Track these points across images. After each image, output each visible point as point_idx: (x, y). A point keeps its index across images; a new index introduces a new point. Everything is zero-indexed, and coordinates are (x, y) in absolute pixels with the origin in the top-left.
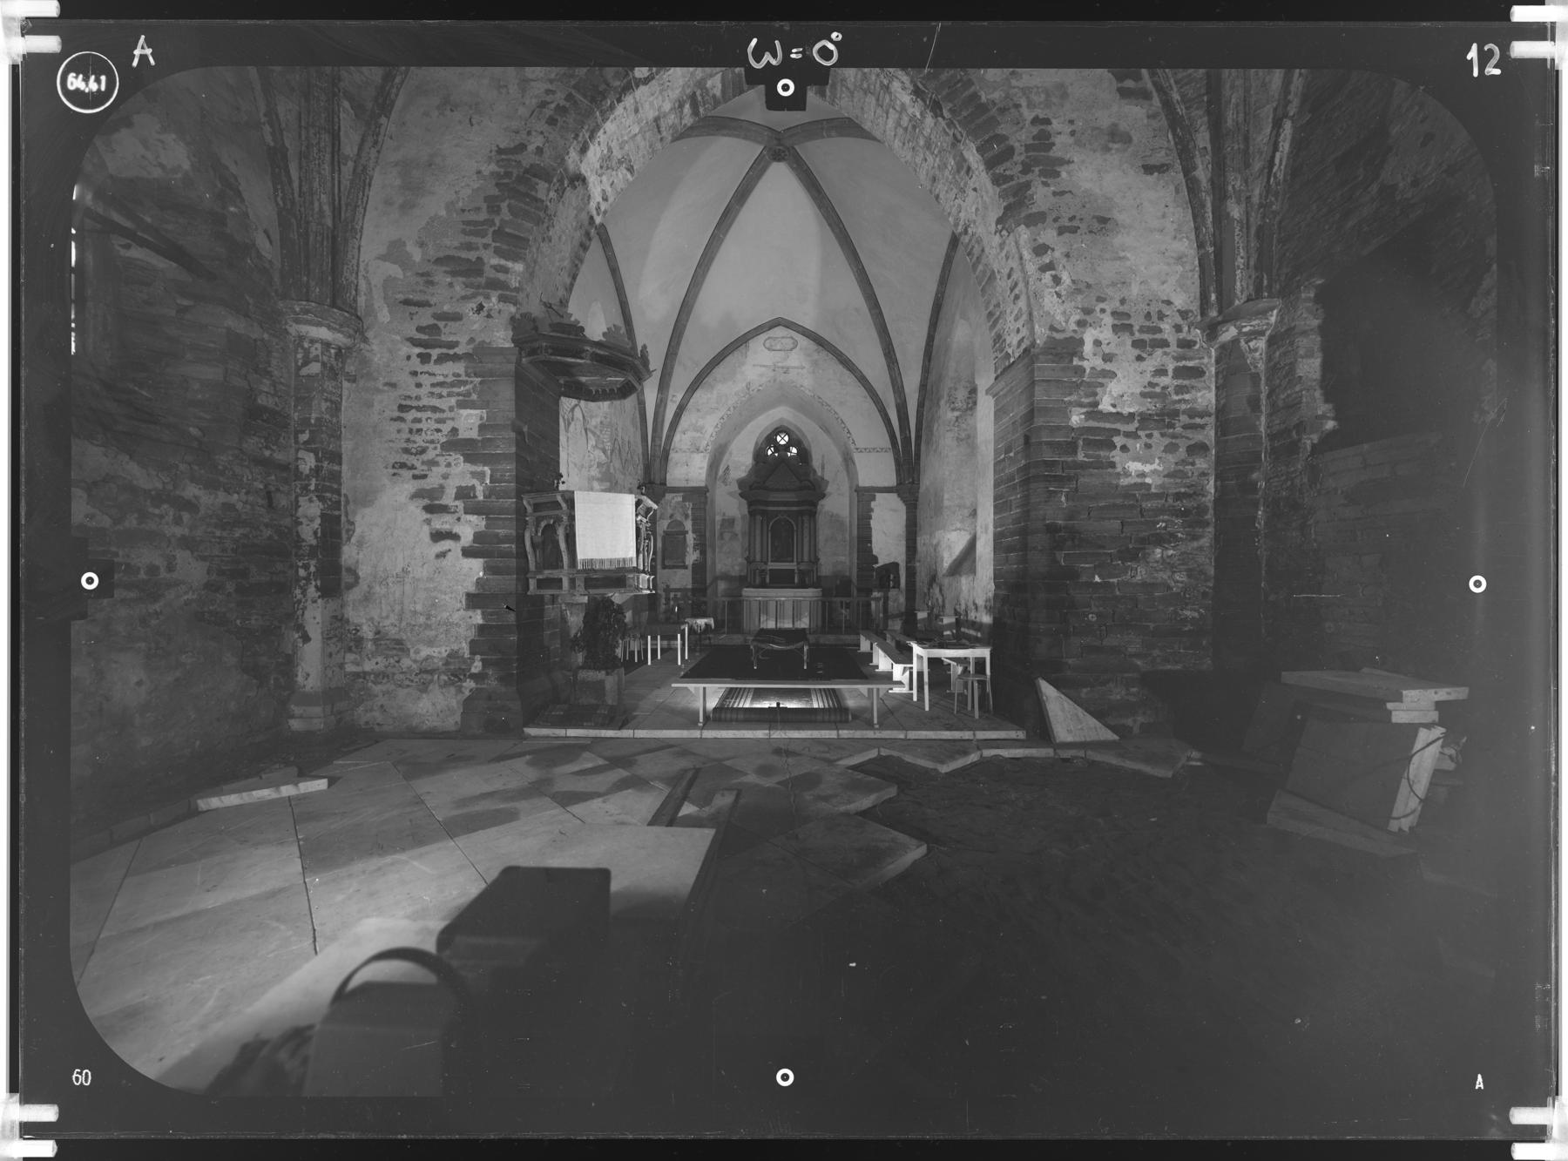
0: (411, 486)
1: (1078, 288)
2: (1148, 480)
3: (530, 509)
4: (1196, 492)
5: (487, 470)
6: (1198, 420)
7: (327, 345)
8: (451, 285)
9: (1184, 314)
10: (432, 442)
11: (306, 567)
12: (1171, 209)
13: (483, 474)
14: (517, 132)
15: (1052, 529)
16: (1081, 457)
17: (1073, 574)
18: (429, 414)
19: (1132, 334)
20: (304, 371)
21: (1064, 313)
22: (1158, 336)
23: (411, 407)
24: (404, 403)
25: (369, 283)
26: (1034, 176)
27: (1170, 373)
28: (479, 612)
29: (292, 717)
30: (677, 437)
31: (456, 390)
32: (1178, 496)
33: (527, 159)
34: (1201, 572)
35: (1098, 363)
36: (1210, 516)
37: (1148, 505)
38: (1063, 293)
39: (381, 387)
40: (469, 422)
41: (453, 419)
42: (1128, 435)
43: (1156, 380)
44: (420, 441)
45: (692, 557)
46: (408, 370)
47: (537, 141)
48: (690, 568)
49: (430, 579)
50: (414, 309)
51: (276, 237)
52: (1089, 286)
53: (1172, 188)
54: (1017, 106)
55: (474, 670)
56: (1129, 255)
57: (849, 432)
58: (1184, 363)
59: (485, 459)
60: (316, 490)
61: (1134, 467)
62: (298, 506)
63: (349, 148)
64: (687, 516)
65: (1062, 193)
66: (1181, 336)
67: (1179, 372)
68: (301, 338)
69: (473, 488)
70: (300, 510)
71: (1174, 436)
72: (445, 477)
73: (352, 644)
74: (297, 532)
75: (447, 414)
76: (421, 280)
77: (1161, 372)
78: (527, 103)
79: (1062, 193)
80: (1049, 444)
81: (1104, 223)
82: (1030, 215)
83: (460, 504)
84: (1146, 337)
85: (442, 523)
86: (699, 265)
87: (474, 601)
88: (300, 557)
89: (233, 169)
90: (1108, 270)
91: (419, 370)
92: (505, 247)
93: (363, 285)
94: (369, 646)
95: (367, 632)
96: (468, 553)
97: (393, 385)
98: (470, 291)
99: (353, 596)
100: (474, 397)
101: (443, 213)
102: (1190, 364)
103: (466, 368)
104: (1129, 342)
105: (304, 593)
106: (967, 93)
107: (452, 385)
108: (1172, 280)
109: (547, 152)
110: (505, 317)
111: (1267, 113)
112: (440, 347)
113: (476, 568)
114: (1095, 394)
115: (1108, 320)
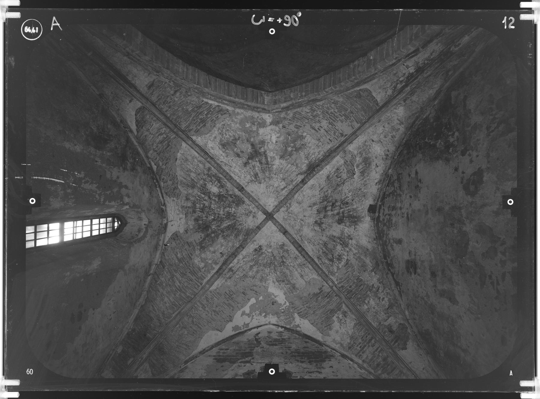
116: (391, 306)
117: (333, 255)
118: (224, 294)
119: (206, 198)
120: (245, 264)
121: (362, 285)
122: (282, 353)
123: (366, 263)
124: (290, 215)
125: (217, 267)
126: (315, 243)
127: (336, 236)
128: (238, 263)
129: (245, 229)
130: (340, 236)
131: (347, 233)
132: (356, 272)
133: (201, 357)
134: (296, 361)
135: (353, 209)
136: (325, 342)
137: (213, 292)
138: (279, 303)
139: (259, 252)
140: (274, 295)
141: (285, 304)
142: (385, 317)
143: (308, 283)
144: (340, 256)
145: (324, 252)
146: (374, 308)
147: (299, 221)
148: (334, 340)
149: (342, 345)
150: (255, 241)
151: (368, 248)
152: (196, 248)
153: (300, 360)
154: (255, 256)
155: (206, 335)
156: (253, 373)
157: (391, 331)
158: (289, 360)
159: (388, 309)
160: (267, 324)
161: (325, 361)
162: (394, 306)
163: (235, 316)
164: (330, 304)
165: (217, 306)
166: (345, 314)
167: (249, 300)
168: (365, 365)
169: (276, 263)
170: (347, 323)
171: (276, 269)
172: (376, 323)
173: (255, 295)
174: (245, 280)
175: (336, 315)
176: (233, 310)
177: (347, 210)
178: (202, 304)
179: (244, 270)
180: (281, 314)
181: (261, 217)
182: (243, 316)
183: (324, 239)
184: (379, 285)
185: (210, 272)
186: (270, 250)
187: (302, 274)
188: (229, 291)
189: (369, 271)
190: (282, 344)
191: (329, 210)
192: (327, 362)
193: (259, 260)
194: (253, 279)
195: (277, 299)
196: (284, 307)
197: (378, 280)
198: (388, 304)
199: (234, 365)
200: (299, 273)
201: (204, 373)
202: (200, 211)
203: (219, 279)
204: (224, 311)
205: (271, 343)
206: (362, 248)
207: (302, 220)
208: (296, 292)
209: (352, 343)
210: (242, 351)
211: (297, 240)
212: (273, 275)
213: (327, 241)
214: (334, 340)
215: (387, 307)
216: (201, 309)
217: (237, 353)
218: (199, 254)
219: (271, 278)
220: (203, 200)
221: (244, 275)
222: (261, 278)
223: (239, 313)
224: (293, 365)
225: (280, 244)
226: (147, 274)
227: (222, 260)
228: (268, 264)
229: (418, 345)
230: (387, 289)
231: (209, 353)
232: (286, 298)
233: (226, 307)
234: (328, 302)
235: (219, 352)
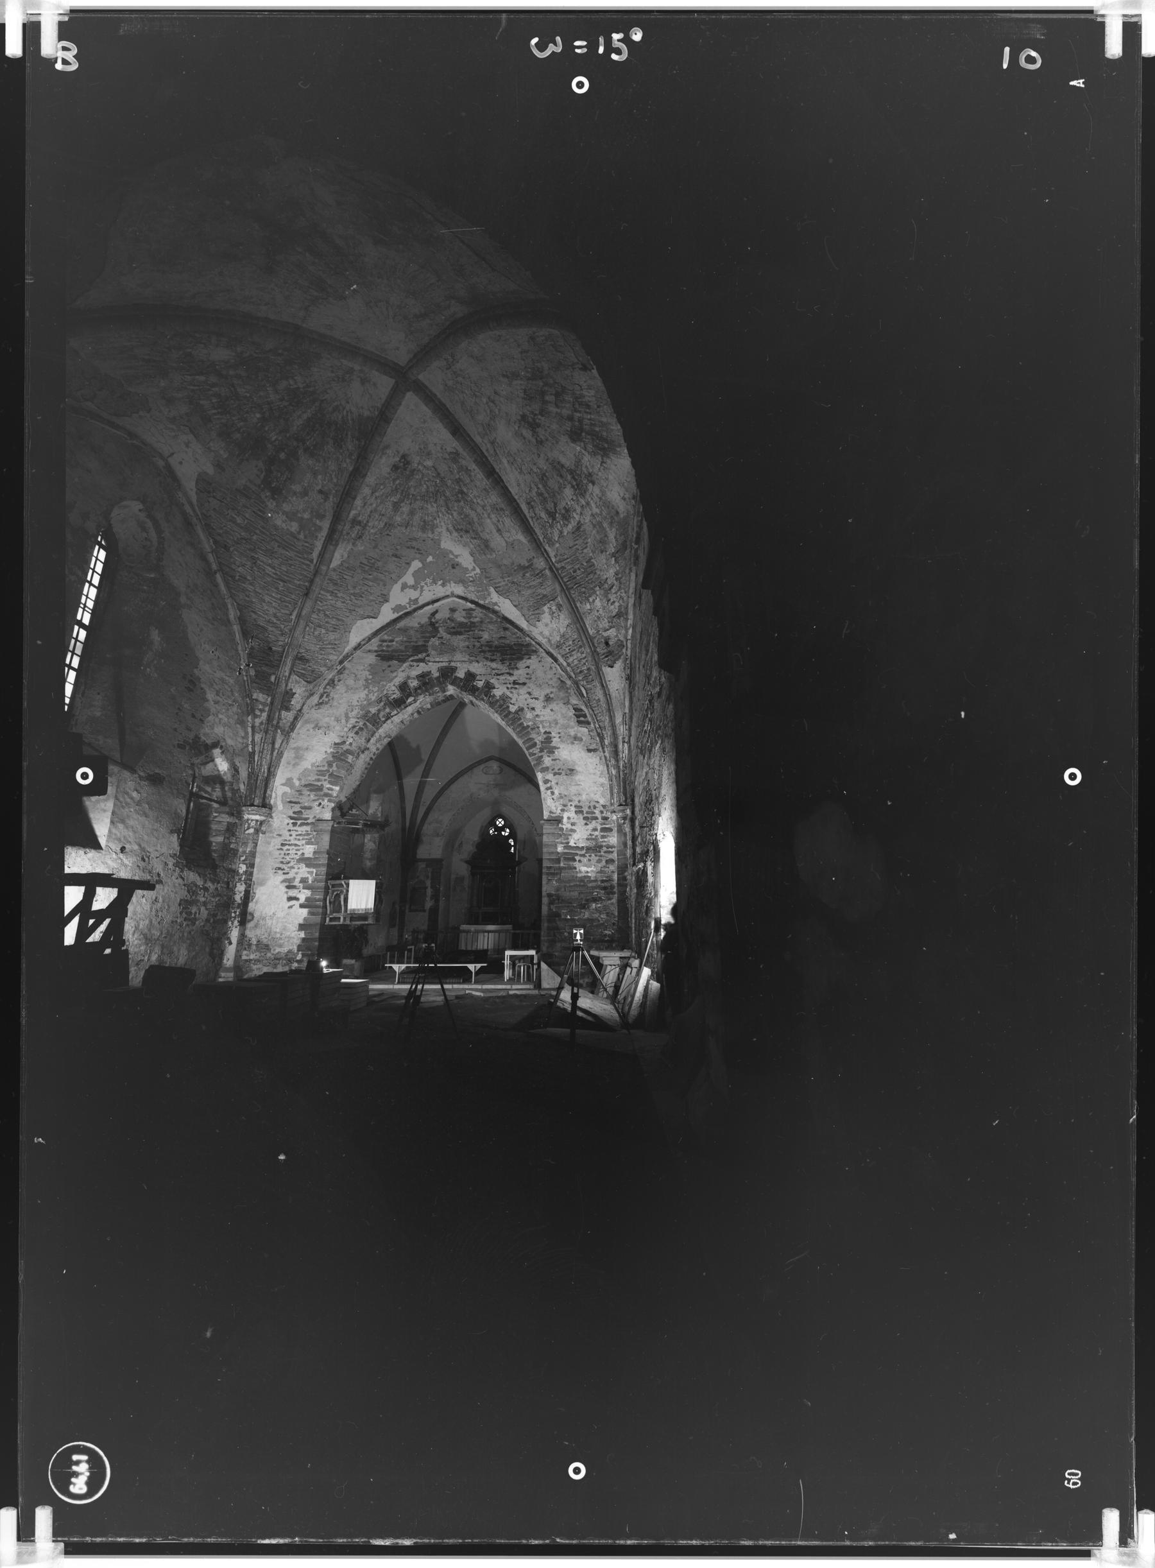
0: (281, 877)
1: (561, 797)
2: (589, 875)
3: (330, 887)
4: (610, 880)
5: (314, 870)
6: (610, 849)
7: (257, 821)
8: (309, 795)
9: (604, 806)
10: (293, 859)
11: (235, 912)
12: (599, 766)
13: (312, 872)
14: (343, 737)
15: (549, 895)
16: (562, 865)
17: (558, 915)
18: (293, 847)
19: (583, 814)
20: (247, 832)
21: (555, 806)
22: (593, 815)
23: (286, 844)
24: (284, 842)
25: (276, 794)
26: (544, 754)
27: (599, 830)
28: (303, 932)
29: (220, 977)
30: (425, 828)
31: (306, 837)
32: (602, 881)
33: (346, 747)
34: (612, 914)
35: (569, 826)
36: (615, 890)
37: (590, 885)
38: (555, 798)
39: (275, 836)
40: (309, 851)
41: (303, 849)
42: (581, 855)
43: (593, 833)
44: (288, 858)
45: (429, 904)
46: (287, 829)
47: (351, 740)
48: (427, 911)
49: (284, 917)
50: (293, 805)
51: (246, 783)
52: (565, 796)
53: (598, 758)
54: (538, 727)
55: (298, 958)
56: (581, 783)
57: (533, 824)
58: (604, 826)
59: (314, 866)
60: (245, 880)
61: (584, 869)
62: (236, 887)
63: (277, 746)
64: (428, 877)
65: (555, 760)
66: (603, 815)
67: (603, 830)
68: (248, 820)
69: (308, 878)
70: (237, 888)
71: (601, 856)
72: (297, 873)
73: (247, 947)
74: (234, 898)
75: (303, 847)
76: (297, 793)
77: (595, 830)
78: (348, 726)
79: (555, 760)
80: (549, 859)
81: (571, 771)
82: (543, 768)
83: (301, 885)
84: (589, 816)
85: (292, 893)
86: (441, 734)
87: (302, 927)
88: (233, 908)
89: (238, 765)
90: (573, 790)
91: (292, 829)
92: (333, 780)
93: (274, 795)
94: (254, 947)
95: (254, 941)
96: (302, 906)
97: (280, 835)
98: (316, 798)
99: (250, 925)
100: (313, 840)
101: (310, 767)
102: (607, 826)
103: (311, 828)
104: (582, 818)
105: (232, 924)
106: (519, 723)
107: (304, 835)
108: (599, 793)
109: (354, 745)
110: (330, 808)
111: (621, 738)
112: (301, 820)
113: (305, 911)
114: (568, 839)
115: (573, 809)
116: (619, 615)
117: (555, 504)
118: (360, 566)
119: (213, 379)
120: (381, 503)
121: (592, 572)
122: (468, 647)
123: (608, 537)
124: (460, 379)
125: (326, 525)
126: (523, 468)
127: (566, 466)
128: (365, 504)
129: (353, 420)
130: (573, 467)
131: (586, 467)
132: (588, 549)
133: (358, 652)
134: (484, 659)
135: (601, 422)
136: (530, 631)
137: (339, 568)
138: (465, 566)
139: (405, 470)
140: (453, 554)
141: (474, 569)
142: (607, 626)
143: (511, 545)
144: (567, 511)
145: (540, 494)
146: (598, 611)
147: (485, 400)
148: (541, 633)
149: (549, 641)
150: (387, 447)
151: (619, 510)
152: (263, 496)
153: (489, 657)
154: (398, 482)
155: (354, 627)
156: (428, 675)
157: (607, 644)
158: (476, 657)
159: (614, 617)
160: (447, 597)
161: (522, 659)
162: (623, 616)
163: (391, 593)
164: (543, 587)
165: (354, 588)
166: (559, 607)
167: (409, 564)
168: (568, 669)
169: (448, 494)
170: (561, 618)
171: (450, 505)
172: (593, 631)
173: (418, 556)
174: (391, 534)
175: (548, 605)
176: (385, 585)
177: (588, 419)
178: (328, 591)
179: (383, 515)
180: (470, 583)
181: (384, 384)
182: (405, 590)
183: (542, 464)
184: (615, 582)
185: (317, 537)
186: (429, 463)
187: (500, 527)
188: (367, 558)
189: (608, 553)
190: (469, 631)
191: (550, 402)
192: (524, 661)
193: (409, 488)
194: (406, 527)
195: (459, 560)
196: (472, 574)
197: (616, 574)
198: (617, 610)
199: (405, 665)
200: (494, 524)
201: (369, 675)
202: (218, 413)
203: (340, 546)
204: (369, 590)
205: (452, 630)
206: (608, 507)
207: (493, 402)
208: (491, 555)
209: (562, 641)
210: (412, 644)
211: (484, 451)
212: (446, 518)
213: (546, 470)
214: (541, 633)
215: (614, 614)
216: (330, 598)
217: (406, 647)
218: (277, 506)
219: (443, 524)
220: (208, 387)
221: (386, 524)
222: (422, 523)
223: (397, 587)
224: (480, 664)
225: (449, 450)
226: (210, 574)
227: (329, 506)
228: (431, 495)
229: (624, 668)
230: (623, 591)
231: (368, 647)
232: (474, 561)
233: (371, 583)
234: (541, 584)
235: (381, 645)
